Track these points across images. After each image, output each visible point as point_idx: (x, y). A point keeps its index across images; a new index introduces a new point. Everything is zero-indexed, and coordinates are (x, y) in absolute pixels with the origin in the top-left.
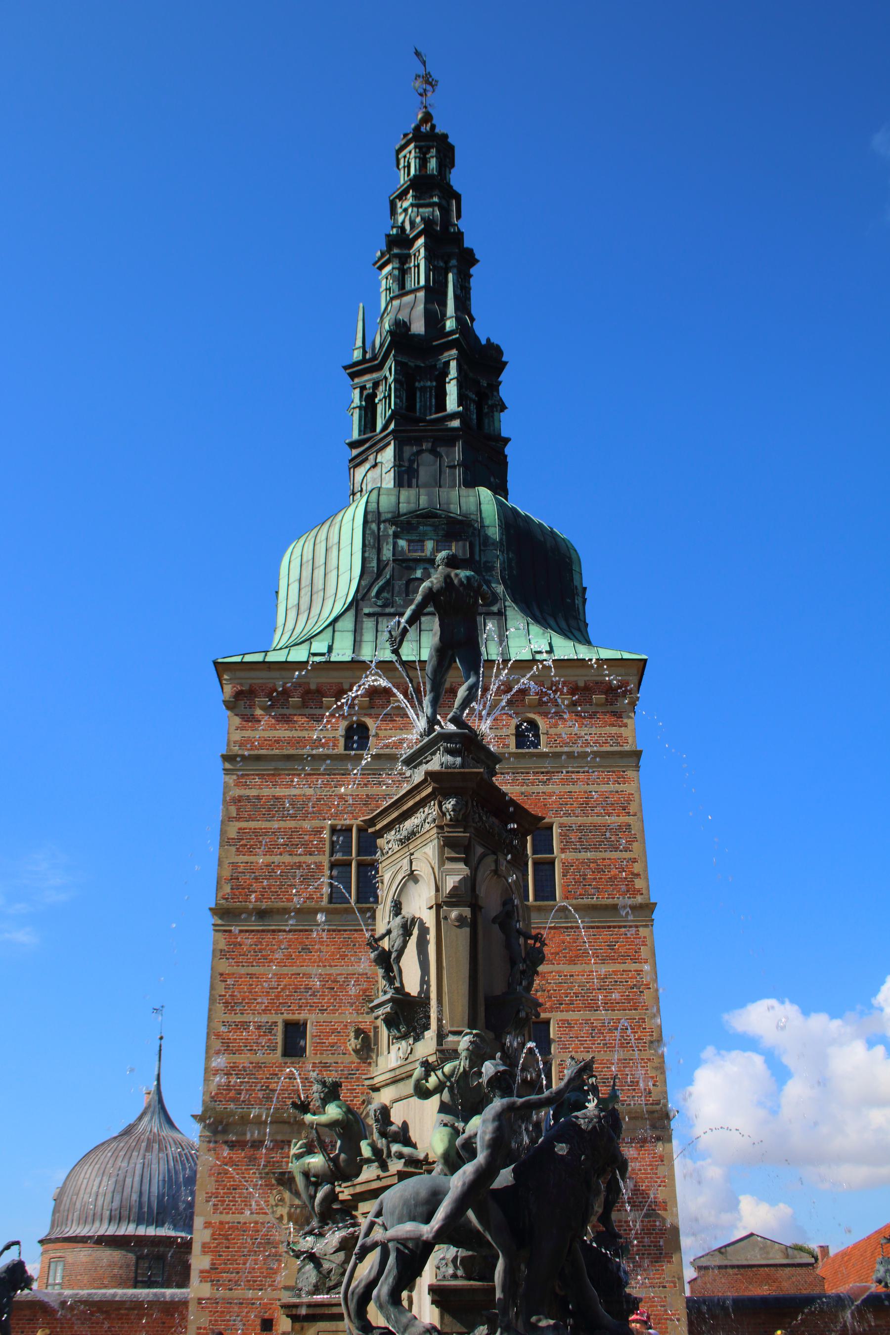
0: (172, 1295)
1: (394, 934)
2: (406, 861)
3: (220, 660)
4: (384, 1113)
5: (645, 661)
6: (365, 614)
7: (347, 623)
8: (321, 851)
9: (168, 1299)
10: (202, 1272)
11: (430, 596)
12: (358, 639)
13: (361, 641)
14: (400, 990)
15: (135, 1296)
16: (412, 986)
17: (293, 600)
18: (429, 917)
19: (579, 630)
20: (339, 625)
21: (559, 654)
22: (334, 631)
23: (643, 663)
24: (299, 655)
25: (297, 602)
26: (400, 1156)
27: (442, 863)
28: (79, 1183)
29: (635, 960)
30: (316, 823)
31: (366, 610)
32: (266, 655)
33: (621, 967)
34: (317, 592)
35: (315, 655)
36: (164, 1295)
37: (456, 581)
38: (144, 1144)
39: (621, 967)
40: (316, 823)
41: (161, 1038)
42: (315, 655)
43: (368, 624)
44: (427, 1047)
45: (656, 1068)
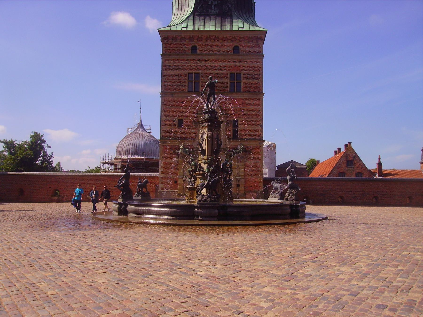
0: (153, 175)
1: (201, 140)
2: (203, 130)
3: (159, 29)
4: (200, 164)
5: (267, 31)
6: (196, 15)
7: (192, 18)
8: (186, 79)
9: (152, 175)
10: (162, 172)
11: (208, 85)
12: (194, 22)
13: (195, 23)
14: (202, 149)
15: (145, 175)
16: (204, 148)
17: (177, 7)
18: (206, 138)
19: (252, 17)
20: (189, 18)
21: (246, 29)
22: (188, 20)
23: (266, 32)
24: (179, 28)
25: (178, 7)
26: (202, 171)
27: (208, 132)
28: (123, 145)
29: (258, 106)
30: (184, 72)
31: (196, 14)
32: (171, 27)
33: (255, 108)
34: (183, 6)
35: (183, 28)
36: (151, 175)
37: (208, 118)
38: (139, 136)
39: (255, 108)
40: (184, 72)
41: (141, 108)
42: (183, 28)
43: (197, 18)
44: (206, 157)
45: (261, 131)
